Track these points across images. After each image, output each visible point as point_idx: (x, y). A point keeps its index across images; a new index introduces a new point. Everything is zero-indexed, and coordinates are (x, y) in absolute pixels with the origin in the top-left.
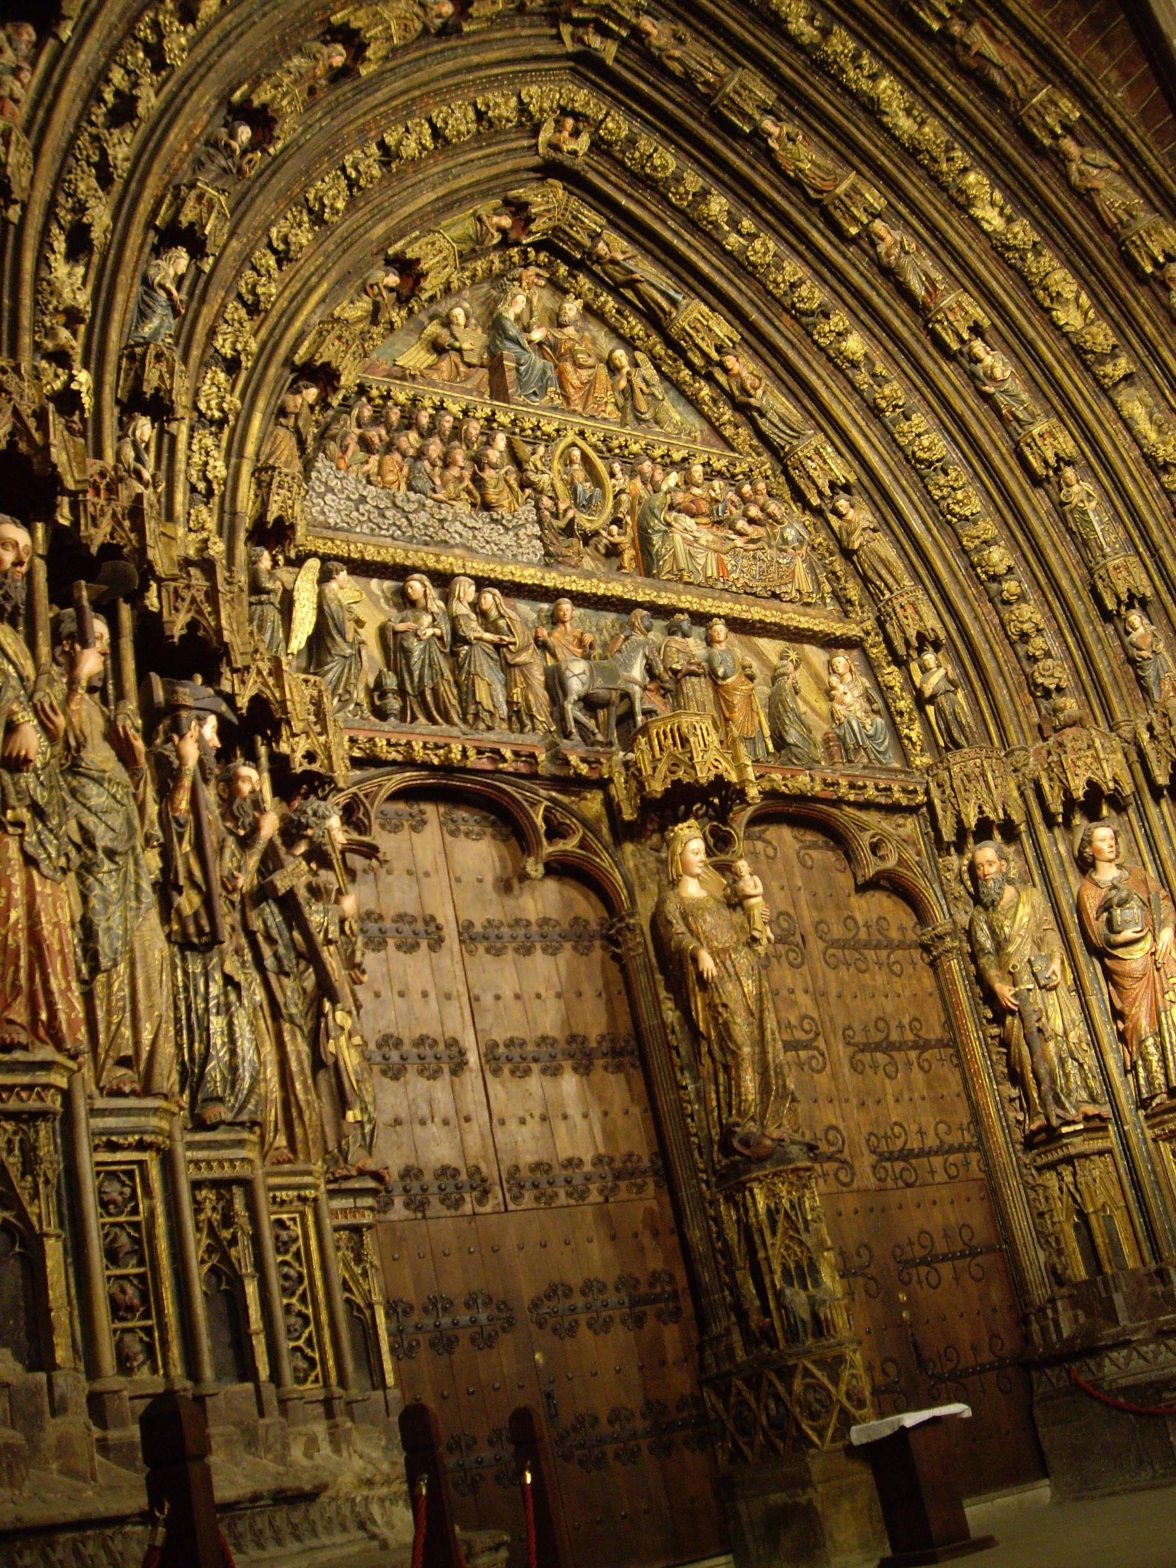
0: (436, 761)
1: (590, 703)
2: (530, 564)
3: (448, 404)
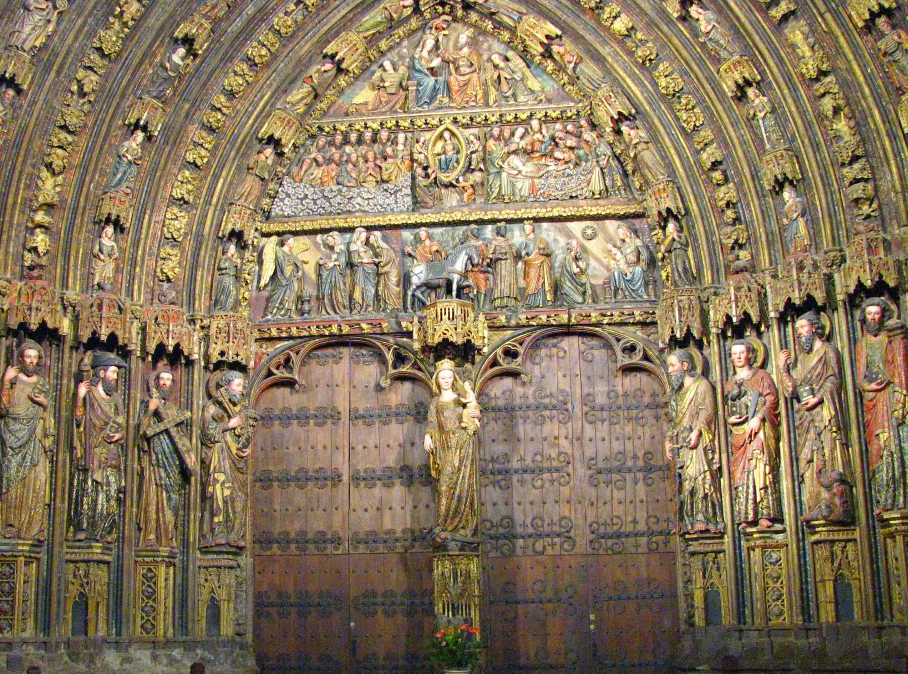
0: (327, 333)
1: (429, 286)
2: (401, 212)
3: (369, 124)
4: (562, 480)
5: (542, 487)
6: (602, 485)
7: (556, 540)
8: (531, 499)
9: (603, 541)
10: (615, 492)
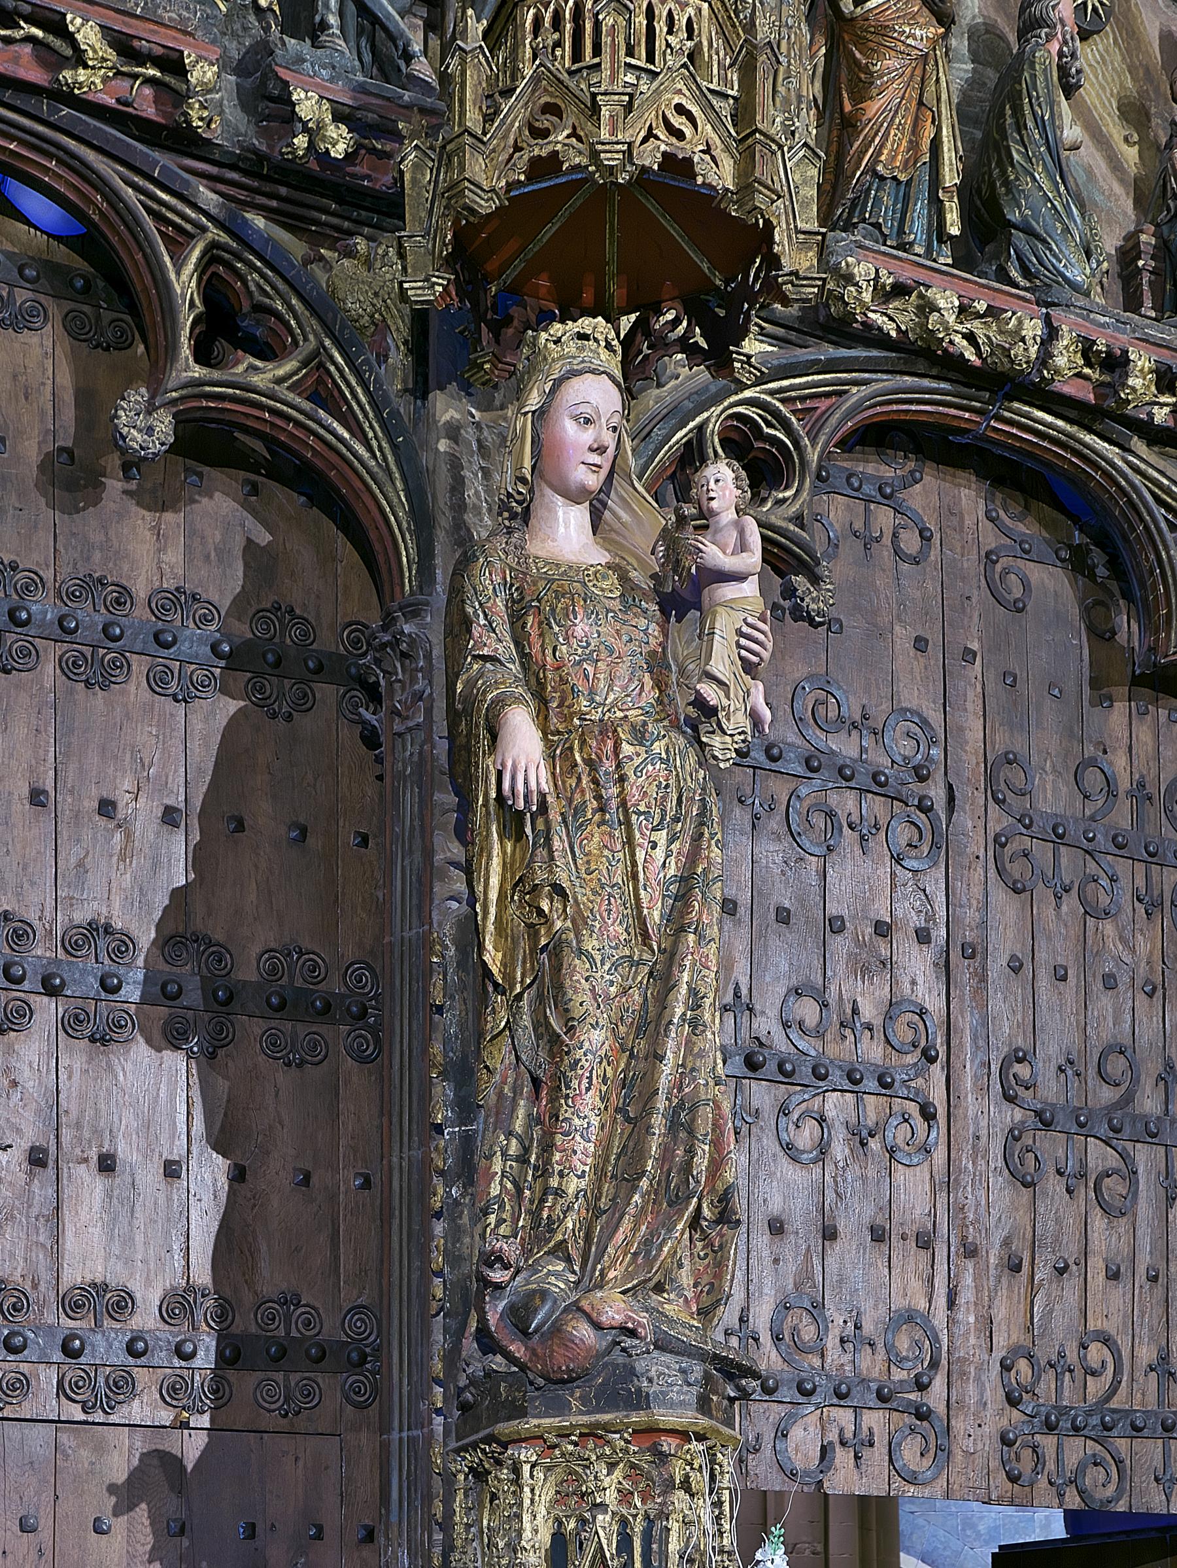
4: (899, 1134)
5: (823, 1149)
6: (1054, 1185)
7: (874, 1420)
8: (776, 1205)
9: (1048, 1443)
10: (1098, 1222)
